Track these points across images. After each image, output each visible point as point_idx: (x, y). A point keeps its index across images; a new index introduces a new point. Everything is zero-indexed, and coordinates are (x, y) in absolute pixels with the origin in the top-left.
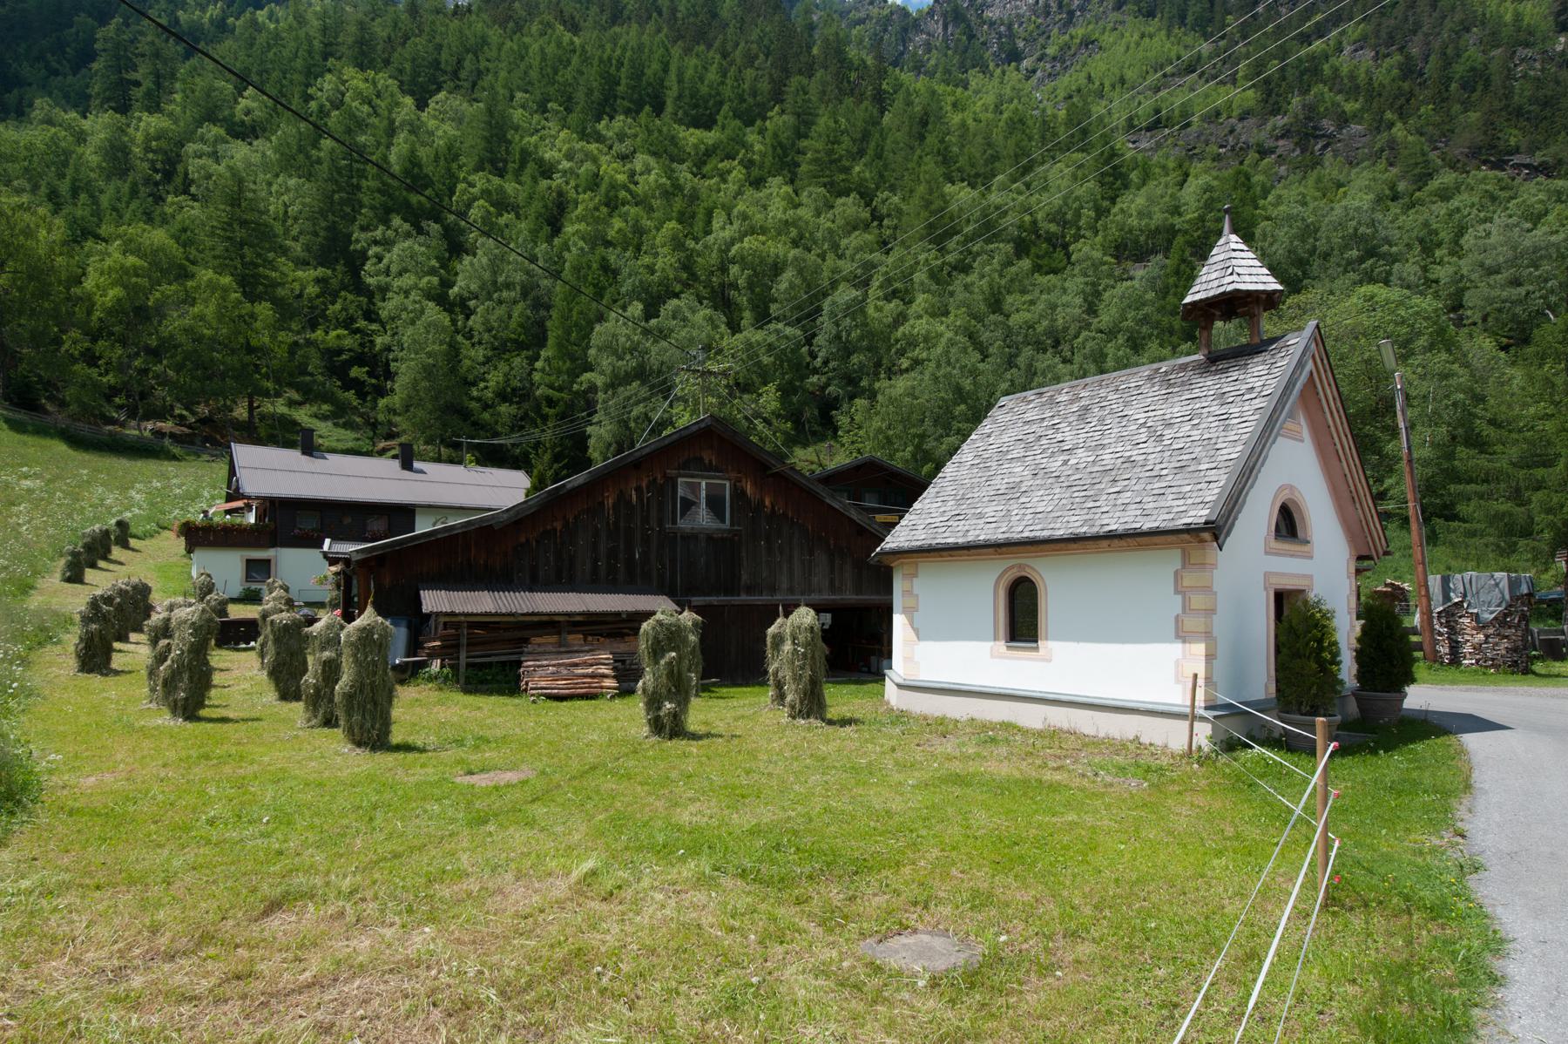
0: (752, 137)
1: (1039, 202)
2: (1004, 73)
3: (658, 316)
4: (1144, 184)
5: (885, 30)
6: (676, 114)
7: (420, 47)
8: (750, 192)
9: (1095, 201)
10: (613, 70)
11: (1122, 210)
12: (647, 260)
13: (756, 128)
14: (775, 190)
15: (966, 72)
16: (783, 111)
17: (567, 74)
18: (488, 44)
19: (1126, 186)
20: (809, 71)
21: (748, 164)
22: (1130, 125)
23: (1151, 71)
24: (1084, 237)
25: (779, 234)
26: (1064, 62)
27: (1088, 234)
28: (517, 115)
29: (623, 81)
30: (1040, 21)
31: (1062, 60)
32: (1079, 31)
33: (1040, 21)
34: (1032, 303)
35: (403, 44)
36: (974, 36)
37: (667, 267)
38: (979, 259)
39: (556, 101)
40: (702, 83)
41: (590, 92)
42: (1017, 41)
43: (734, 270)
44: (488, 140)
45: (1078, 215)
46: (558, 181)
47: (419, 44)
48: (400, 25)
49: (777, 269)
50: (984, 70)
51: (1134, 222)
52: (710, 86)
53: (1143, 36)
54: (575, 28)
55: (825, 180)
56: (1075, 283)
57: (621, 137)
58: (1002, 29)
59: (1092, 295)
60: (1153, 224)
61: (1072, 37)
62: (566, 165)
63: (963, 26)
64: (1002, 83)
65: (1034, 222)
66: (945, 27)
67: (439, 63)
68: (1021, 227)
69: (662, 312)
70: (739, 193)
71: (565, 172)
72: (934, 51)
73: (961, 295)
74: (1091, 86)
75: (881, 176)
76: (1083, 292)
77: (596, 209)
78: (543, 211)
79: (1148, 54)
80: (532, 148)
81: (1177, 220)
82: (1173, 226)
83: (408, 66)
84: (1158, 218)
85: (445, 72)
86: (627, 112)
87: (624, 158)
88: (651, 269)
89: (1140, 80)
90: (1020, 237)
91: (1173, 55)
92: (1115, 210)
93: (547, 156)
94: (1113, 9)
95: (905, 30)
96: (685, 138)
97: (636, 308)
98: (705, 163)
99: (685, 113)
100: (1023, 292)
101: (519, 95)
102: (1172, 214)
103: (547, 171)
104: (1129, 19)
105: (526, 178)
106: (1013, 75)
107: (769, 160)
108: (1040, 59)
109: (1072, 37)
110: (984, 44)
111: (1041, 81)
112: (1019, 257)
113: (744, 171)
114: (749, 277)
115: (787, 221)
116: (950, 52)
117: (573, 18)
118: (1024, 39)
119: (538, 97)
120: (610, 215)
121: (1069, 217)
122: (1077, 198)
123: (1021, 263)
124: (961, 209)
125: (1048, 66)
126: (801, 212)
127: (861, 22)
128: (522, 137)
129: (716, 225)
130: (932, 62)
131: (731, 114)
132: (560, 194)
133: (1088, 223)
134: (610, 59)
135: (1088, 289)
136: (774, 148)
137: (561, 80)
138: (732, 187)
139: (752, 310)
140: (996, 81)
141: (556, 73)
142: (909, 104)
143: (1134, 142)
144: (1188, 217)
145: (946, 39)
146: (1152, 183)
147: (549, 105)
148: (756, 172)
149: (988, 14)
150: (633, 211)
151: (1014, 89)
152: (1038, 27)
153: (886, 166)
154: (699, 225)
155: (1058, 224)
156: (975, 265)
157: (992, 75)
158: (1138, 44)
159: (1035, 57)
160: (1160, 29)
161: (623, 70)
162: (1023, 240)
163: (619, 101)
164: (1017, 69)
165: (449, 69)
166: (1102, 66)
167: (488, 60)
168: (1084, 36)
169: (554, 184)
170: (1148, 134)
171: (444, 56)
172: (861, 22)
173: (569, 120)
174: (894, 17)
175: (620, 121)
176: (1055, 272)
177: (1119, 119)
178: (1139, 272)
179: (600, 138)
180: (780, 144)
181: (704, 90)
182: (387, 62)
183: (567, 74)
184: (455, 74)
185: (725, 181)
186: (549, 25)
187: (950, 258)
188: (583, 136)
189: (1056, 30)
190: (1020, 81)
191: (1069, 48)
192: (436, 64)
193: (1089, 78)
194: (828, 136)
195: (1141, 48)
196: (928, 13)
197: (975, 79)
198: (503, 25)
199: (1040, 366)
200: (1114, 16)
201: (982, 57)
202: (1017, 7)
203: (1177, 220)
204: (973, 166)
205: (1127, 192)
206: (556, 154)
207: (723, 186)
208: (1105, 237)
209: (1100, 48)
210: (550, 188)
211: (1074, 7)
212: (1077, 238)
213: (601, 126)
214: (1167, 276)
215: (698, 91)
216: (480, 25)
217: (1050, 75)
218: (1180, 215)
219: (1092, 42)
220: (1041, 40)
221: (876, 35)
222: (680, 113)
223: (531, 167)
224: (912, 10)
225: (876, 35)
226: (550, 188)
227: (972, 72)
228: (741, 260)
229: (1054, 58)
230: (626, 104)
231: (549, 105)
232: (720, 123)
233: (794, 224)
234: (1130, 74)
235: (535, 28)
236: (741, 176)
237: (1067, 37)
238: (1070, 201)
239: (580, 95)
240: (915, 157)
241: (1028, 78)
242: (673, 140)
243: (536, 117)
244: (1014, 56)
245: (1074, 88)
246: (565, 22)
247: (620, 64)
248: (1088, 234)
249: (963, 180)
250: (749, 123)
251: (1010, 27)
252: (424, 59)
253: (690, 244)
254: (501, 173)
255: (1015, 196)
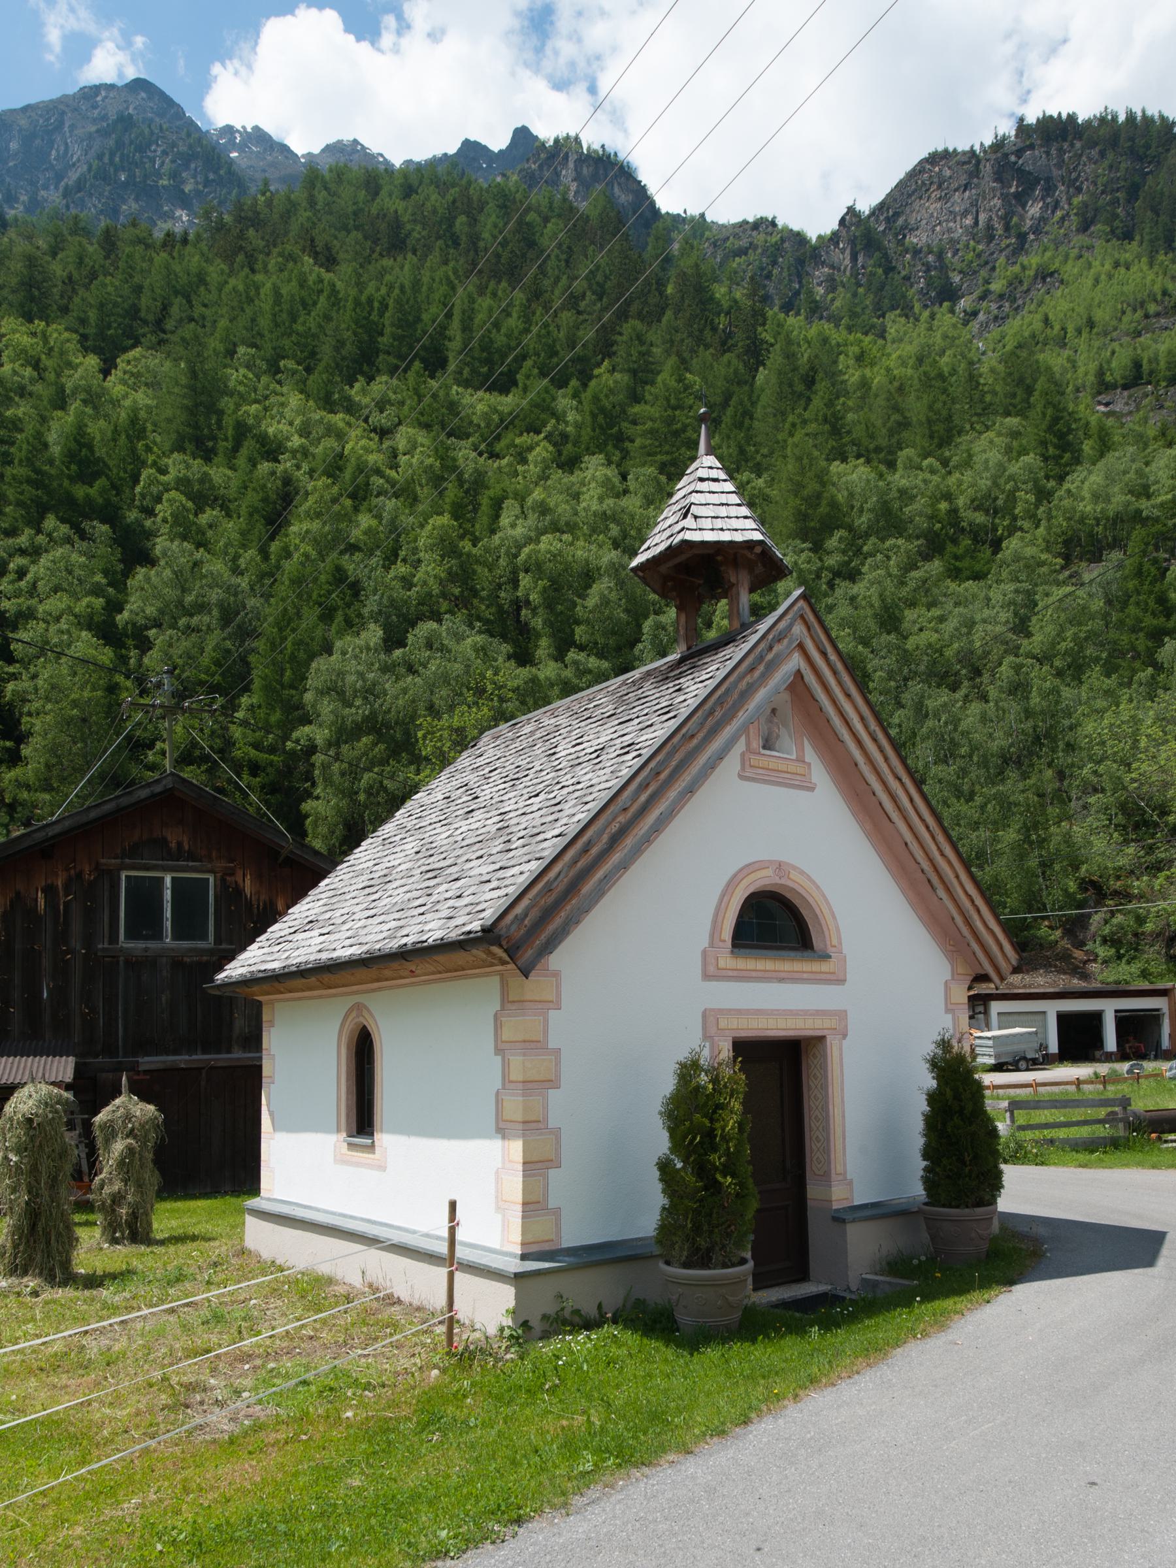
0: (564, 402)
1: (960, 483)
2: (932, 316)
3: (405, 646)
4: (1102, 455)
5: (774, 263)
6: (461, 373)
7: (110, 289)
8: (557, 475)
9: (1036, 481)
10: (374, 317)
11: (1069, 491)
12: (401, 569)
13: (569, 391)
14: (588, 474)
15: (883, 316)
16: (613, 370)
17: (309, 321)
18: (206, 284)
19: (1077, 461)
20: (652, 317)
21: (559, 440)
22: (1103, 386)
23: (1129, 311)
24: (1021, 529)
25: (594, 530)
26: (1015, 300)
27: (1026, 525)
28: (236, 376)
29: (388, 330)
30: (981, 247)
31: (1012, 297)
32: (1033, 260)
33: (981, 247)
34: (942, 619)
35: (87, 287)
36: (893, 269)
37: (431, 581)
38: (869, 560)
39: (294, 357)
40: (499, 331)
41: (341, 343)
42: (951, 274)
43: (525, 580)
44: (192, 411)
45: (1012, 498)
46: (286, 464)
47: (111, 285)
48: (87, 260)
49: (588, 576)
50: (907, 312)
51: (1086, 507)
52: (508, 336)
53: (1117, 265)
54: (329, 261)
55: (665, 458)
56: (1002, 591)
57: (381, 406)
58: (931, 258)
59: (1026, 606)
60: (1112, 509)
61: (1024, 268)
62: (296, 441)
63: (877, 254)
64: (930, 329)
65: (954, 511)
66: (854, 258)
67: (138, 310)
68: (932, 518)
69: (410, 638)
70: (544, 477)
71: (294, 452)
72: (840, 289)
73: (844, 610)
74: (1049, 331)
75: (742, 451)
76: (1012, 603)
77: (335, 501)
78: (260, 505)
79: (1125, 288)
80: (251, 421)
81: (1144, 504)
82: (1139, 512)
83: (93, 315)
84: (1119, 500)
85: (145, 322)
86: (393, 370)
87: (383, 433)
88: (407, 582)
89: (1114, 323)
90: (930, 530)
91: (1157, 289)
92: (1061, 493)
93: (271, 430)
94: (1078, 230)
95: (801, 262)
96: (472, 406)
97: (374, 634)
98: (498, 438)
99: (474, 371)
100: (930, 605)
101: (241, 350)
102: (1138, 496)
103: (271, 450)
104: (1099, 244)
105: (241, 461)
106: (945, 319)
107: (586, 433)
108: (982, 298)
109: (1024, 268)
110: (907, 278)
111: (985, 327)
112: (927, 558)
113: (551, 448)
114: (545, 589)
115: (604, 513)
116: (861, 290)
117: (328, 248)
118: (960, 272)
119: (269, 353)
120: (356, 509)
121: (1000, 502)
122: (1011, 478)
123: (928, 566)
124: (851, 495)
125: (994, 306)
126: (625, 502)
127: (742, 252)
128: (238, 406)
129: (505, 521)
130: (837, 304)
131: (536, 371)
132: (287, 481)
133: (1027, 511)
134: (370, 301)
135: (1020, 598)
136: (594, 416)
137: (300, 328)
138: (533, 469)
139: (553, 635)
140: (923, 326)
141: (294, 319)
142: (790, 356)
143: (1107, 405)
144: (1160, 500)
145: (855, 274)
146: (1111, 457)
147: (282, 363)
148: (569, 449)
149: (913, 239)
150: (390, 504)
151: (945, 337)
152: (979, 256)
153: (748, 439)
154: (483, 520)
155: (987, 512)
156: (865, 569)
157: (917, 320)
158: (1110, 277)
159: (975, 296)
160: (1139, 257)
161: (387, 315)
162: (937, 535)
163: (382, 357)
164: (952, 311)
165: (151, 318)
166: (1064, 306)
167: (205, 306)
168: (1039, 266)
169: (280, 468)
170: (1126, 393)
171: (145, 301)
172: (742, 252)
173: (309, 382)
174: (786, 245)
175: (381, 385)
176: (978, 576)
177: (1086, 369)
178: (1091, 573)
179: (351, 408)
180: (602, 410)
181: (500, 339)
182: (65, 310)
183: (309, 321)
184: (159, 325)
185: (524, 461)
186: (291, 257)
187: (832, 561)
188: (329, 404)
189: (1002, 260)
190: (954, 326)
191: (1021, 282)
192: (134, 312)
193: (1046, 321)
194: (668, 400)
195: (1115, 281)
196: (831, 239)
197: (894, 324)
198: (229, 258)
199: (931, 704)
200: (1079, 240)
201: (904, 296)
202: (950, 230)
203: (1144, 504)
204: (872, 437)
205: (1079, 468)
206: (284, 427)
207: (520, 468)
208: (1049, 529)
209: (1062, 282)
210: (273, 473)
211: (1025, 229)
212: (1012, 530)
213: (355, 392)
214: (1125, 578)
215: (491, 341)
216: (197, 258)
217: (996, 318)
218: (1148, 497)
219: (1051, 274)
220: (983, 273)
221: (762, 269)
222: (466, 371)
223: (249, 447)
224: (812, 235)
225: (762, 269)
226: (273, 473)
227: (890, 316)
228: (535, 567)
229: (1001, 296)
230: (392, 360)
231: (282, 363)
232: (520, 385)
233: (615, 518)
234: (1099, 315)
235: (272, 263)
236: (545, 454)
237: (1017, 269)
238: (1002, 481)
239: (326, 351)
240: (787, 426)
241: (966, 323)
242: (453, 407)
243: (265, 379)
244: (949, 294)
245: (1026, 334)
246: (317, 253)
247: (384, 307)
248: (1026, 525)
249: (858, 457)
250: (561, 382)
251: (940, 256)
252: (116, 305)
253: (466, 545)
254: (208, 456)
255: (928, 476)
